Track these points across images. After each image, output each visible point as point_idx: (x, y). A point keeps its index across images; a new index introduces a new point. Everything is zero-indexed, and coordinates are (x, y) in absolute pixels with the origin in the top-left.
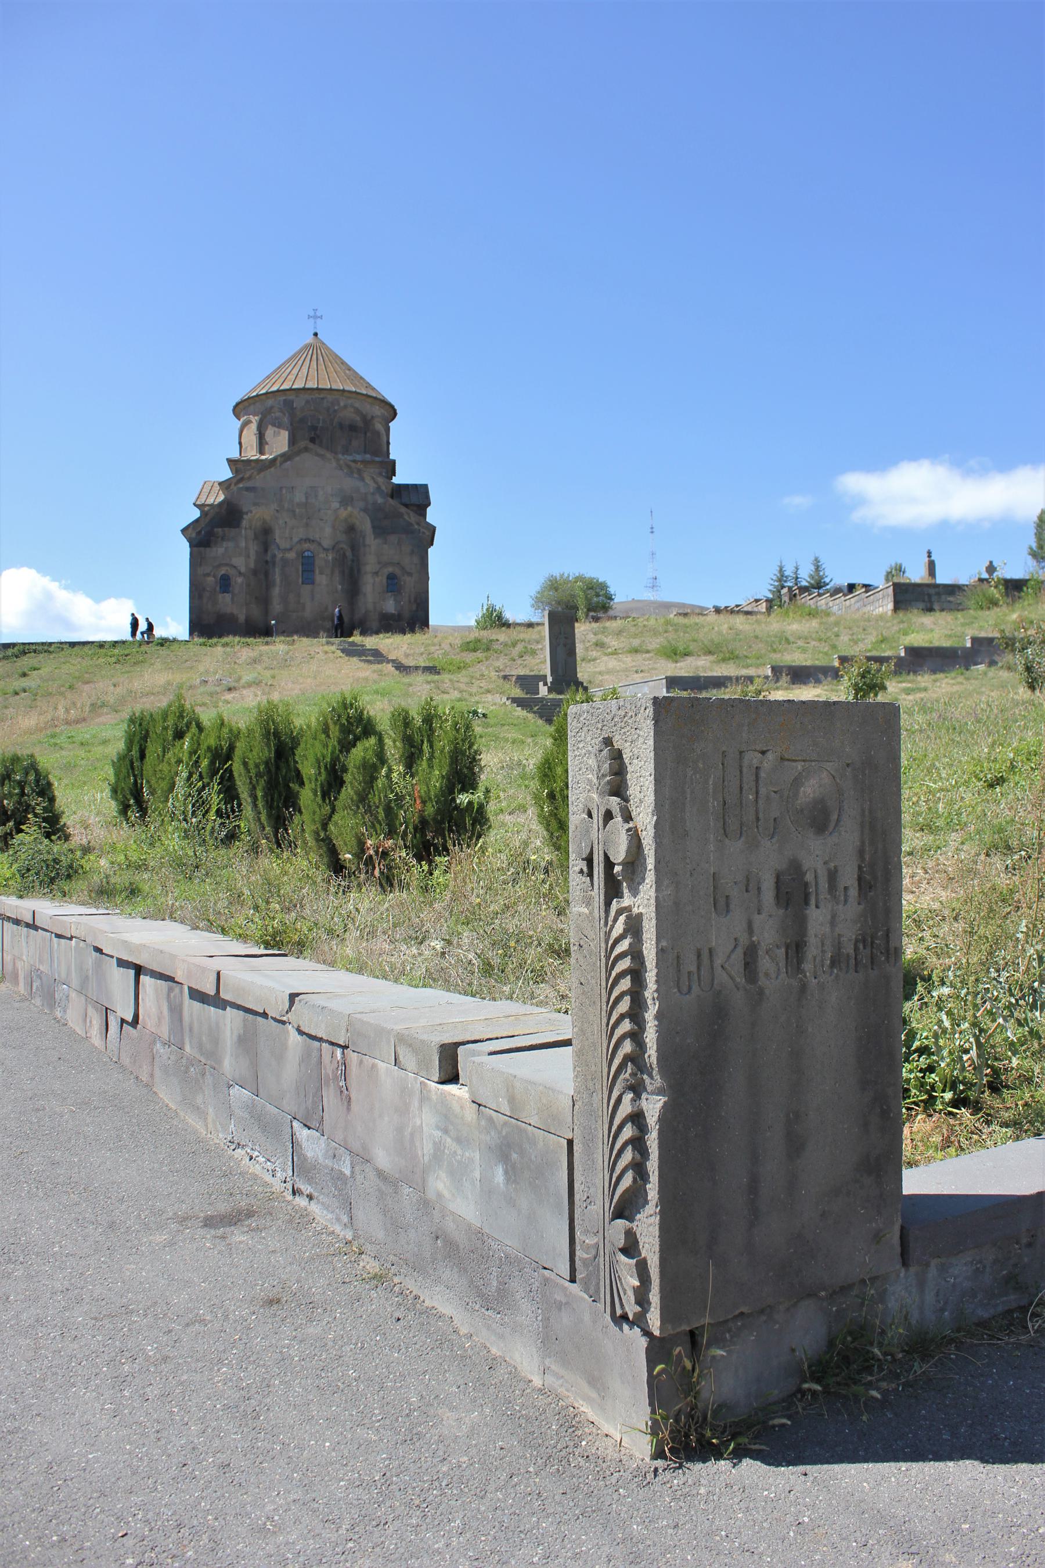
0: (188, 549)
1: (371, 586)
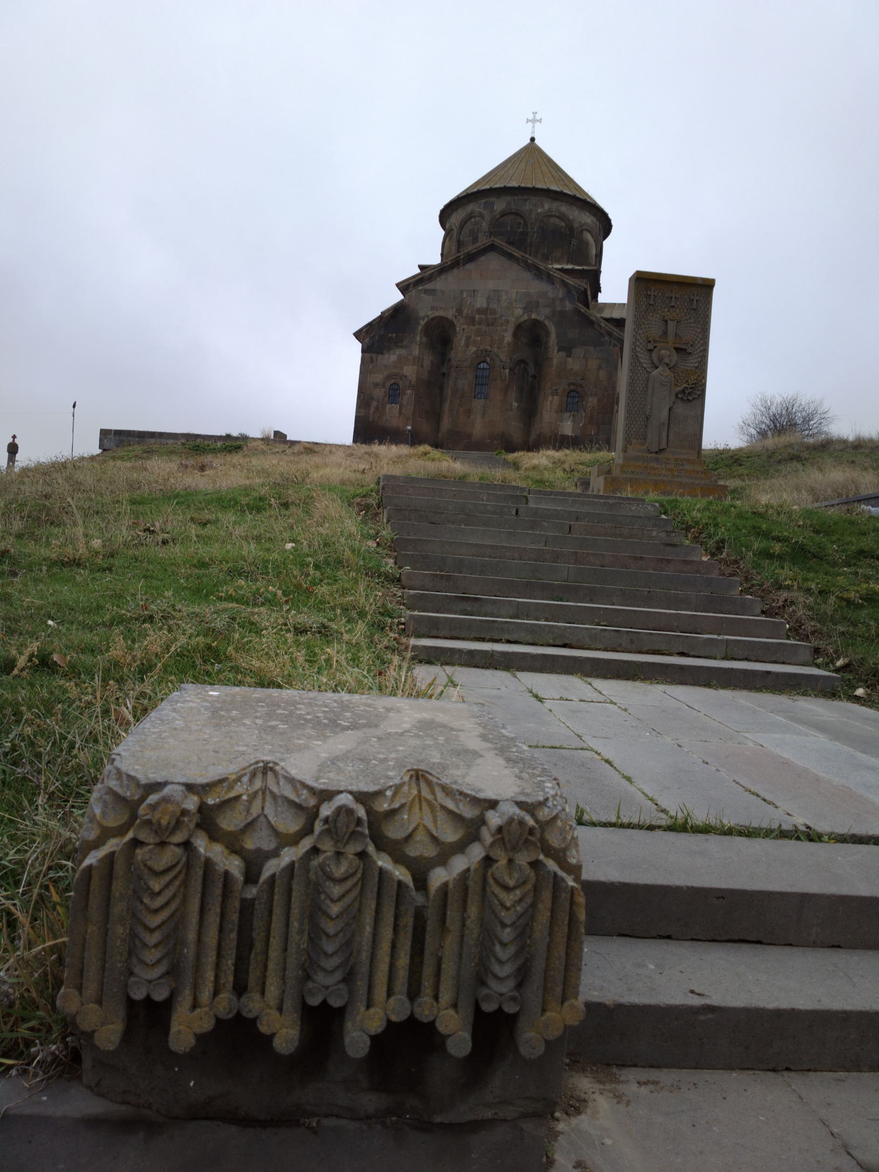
0: (360, 355)
1: (549, 405)
